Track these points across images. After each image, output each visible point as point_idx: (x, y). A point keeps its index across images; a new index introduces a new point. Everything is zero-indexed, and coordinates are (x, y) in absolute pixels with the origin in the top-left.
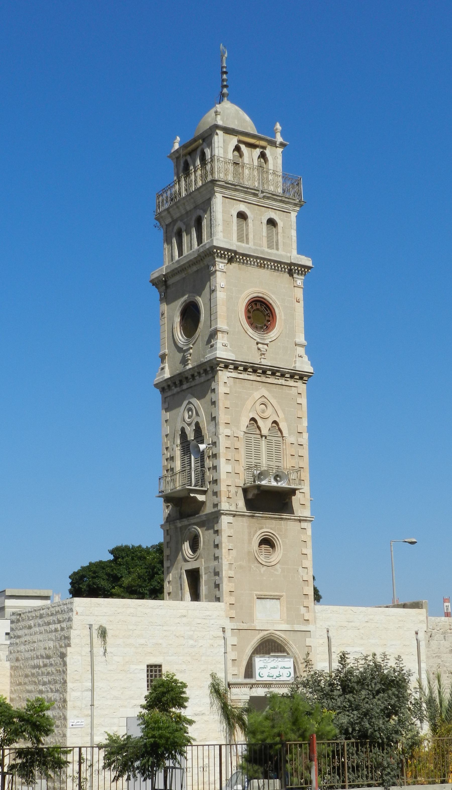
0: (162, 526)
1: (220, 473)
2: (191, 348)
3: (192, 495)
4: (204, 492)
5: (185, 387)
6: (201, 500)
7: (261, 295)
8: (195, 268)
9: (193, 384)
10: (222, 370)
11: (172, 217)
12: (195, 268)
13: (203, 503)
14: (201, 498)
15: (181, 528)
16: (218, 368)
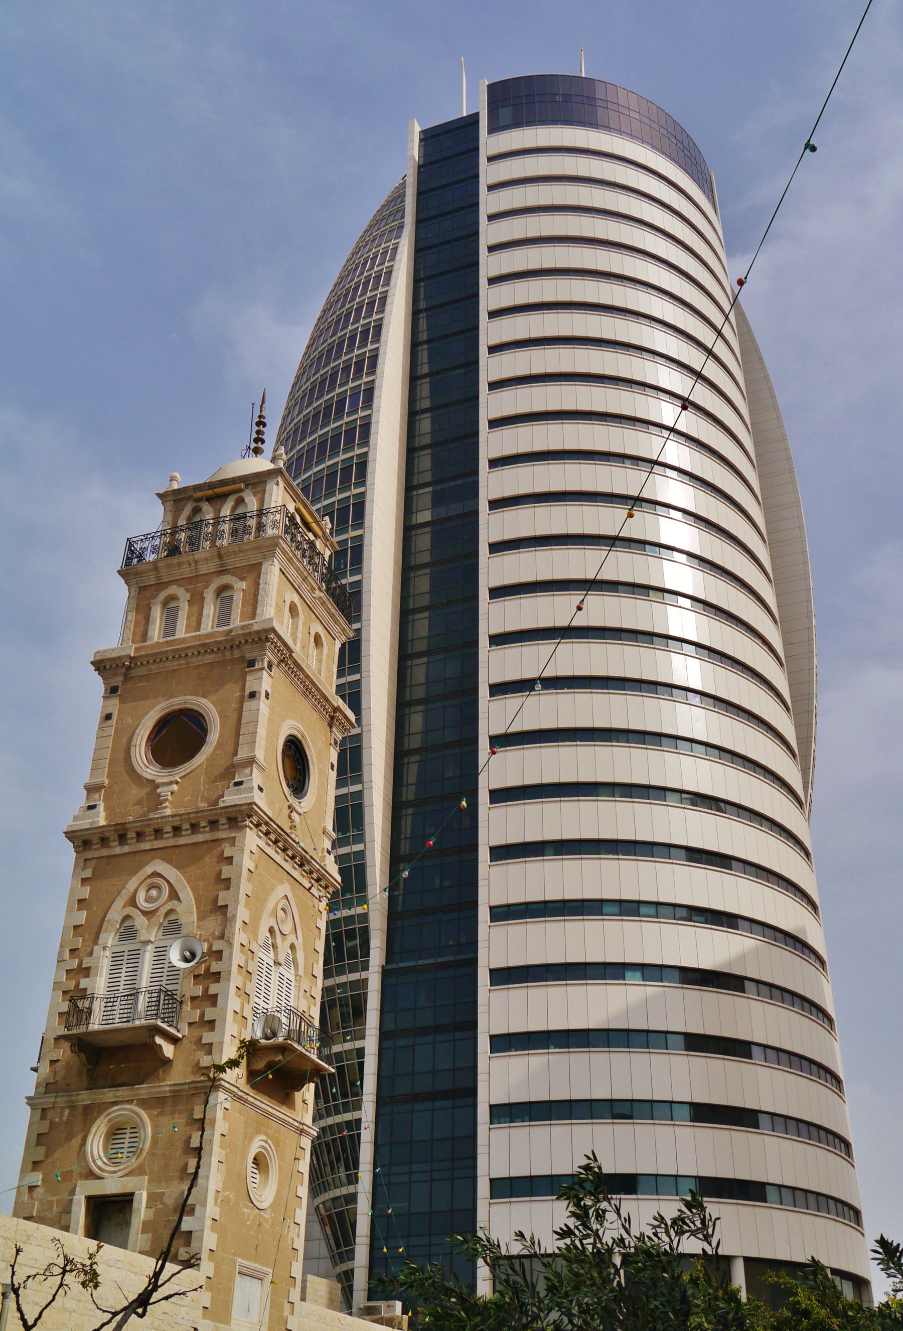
0: (30, 1100)
1: (224, 1010)
2: (177, 783)
3: (159, 1040)
4: (174, 1040)
5: (147, 846)
6: (167, 1055)
7: (300, 736)
8: (209, 658)
9: (171, 842)
10: (251, 829)
11: (159, 578)
12: (209, 658)
13: (167, 1062)
14: (168, 1050)
15: (86, 1107)
16: (248, 823)
